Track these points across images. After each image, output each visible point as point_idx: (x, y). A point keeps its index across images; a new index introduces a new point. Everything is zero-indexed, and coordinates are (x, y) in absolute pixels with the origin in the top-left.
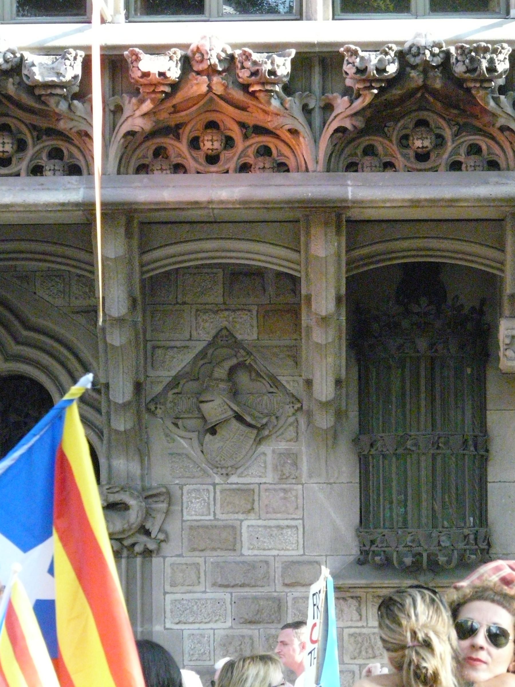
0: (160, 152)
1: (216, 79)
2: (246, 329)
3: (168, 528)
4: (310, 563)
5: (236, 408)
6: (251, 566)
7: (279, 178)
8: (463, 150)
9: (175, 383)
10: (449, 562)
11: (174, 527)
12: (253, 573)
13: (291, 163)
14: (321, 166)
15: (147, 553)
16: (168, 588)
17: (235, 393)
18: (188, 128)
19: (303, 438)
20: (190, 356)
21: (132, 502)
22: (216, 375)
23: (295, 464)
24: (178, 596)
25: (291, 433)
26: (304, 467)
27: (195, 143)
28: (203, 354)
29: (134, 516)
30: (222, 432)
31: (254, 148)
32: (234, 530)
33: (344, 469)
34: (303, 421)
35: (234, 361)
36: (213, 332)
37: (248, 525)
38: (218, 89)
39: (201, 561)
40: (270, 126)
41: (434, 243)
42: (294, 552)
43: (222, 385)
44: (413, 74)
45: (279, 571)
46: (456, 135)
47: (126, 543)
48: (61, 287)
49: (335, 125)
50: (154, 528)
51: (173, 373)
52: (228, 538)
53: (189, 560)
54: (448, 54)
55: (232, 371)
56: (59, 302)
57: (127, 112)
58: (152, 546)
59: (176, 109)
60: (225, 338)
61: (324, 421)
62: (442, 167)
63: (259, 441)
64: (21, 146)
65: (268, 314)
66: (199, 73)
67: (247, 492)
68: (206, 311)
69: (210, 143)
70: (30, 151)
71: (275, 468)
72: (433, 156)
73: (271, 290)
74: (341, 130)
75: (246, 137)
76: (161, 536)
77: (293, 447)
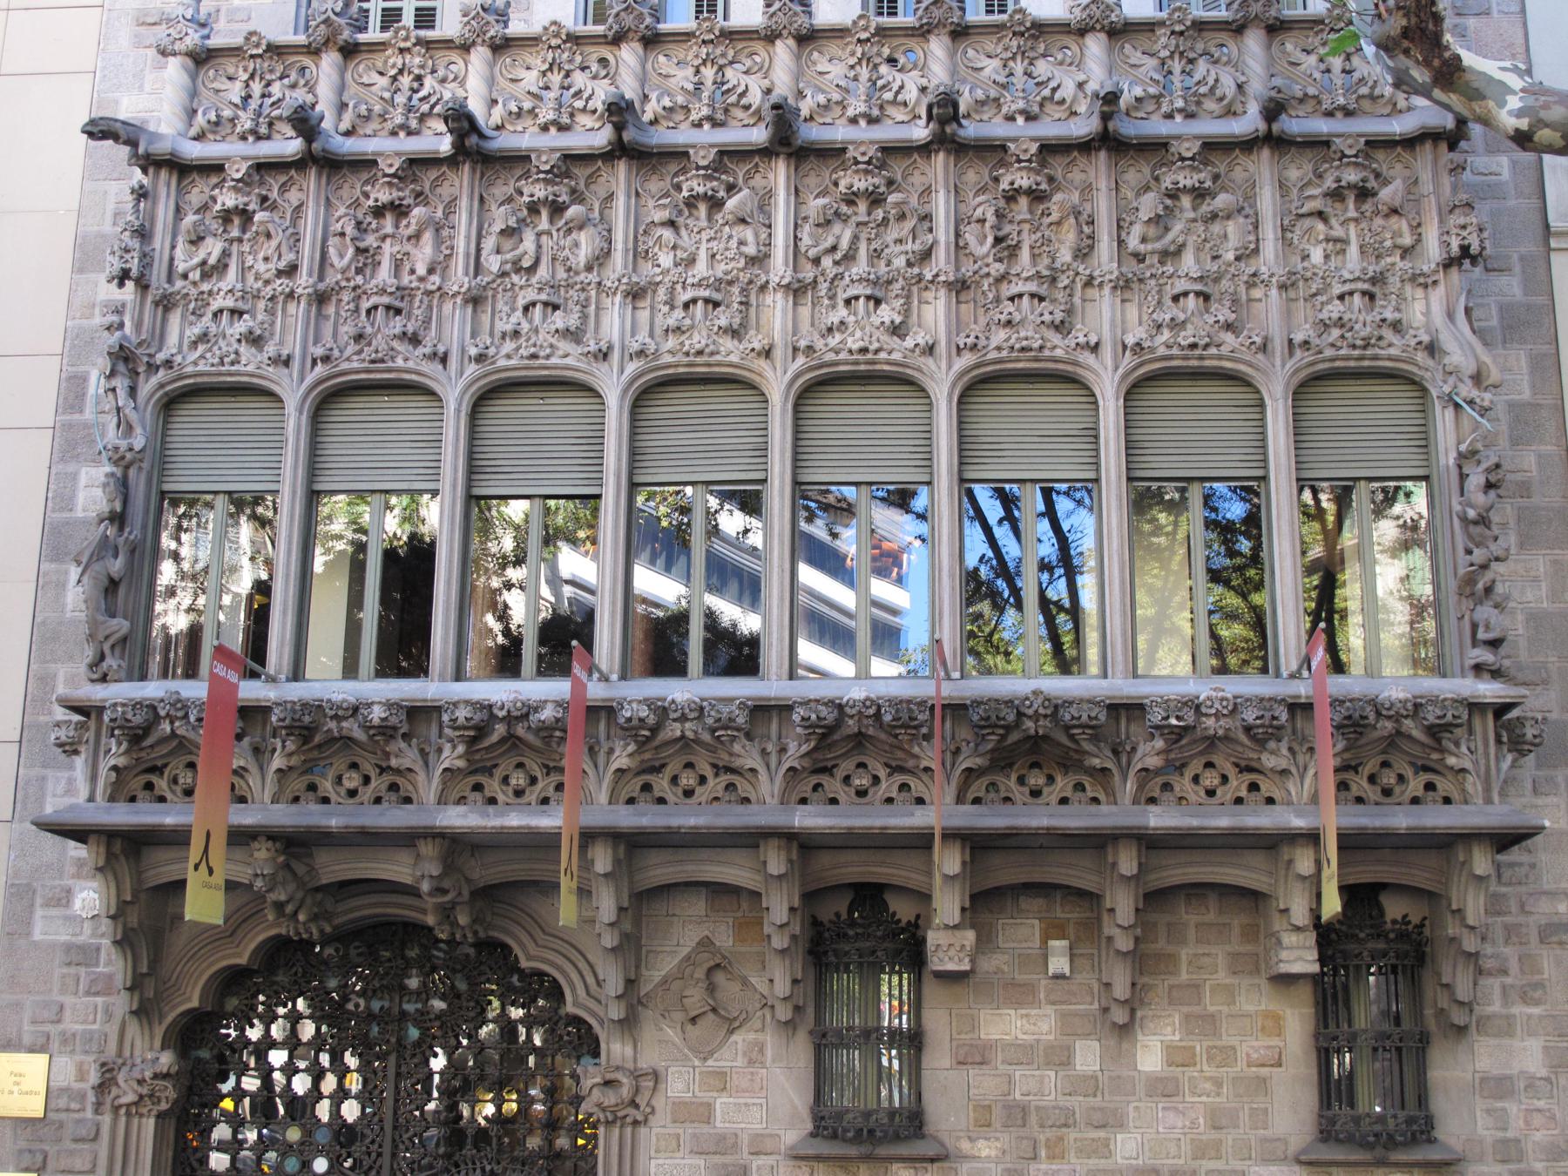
0: (646, 788)
1: (688, 725)
3: (654, 1102)
4: (771, 1135)
6: (722, 1138)
7: (741, 808)
8: (895, 787)
9: (664, 981)
10: (885, 1137)
11: (659, 1102)
12: (724, 1144)
13: (753, 797)
14: (776, 801)
15: (636, 1123)
16: (653, 1154)
17: (712, 989)
19: (768, 1030)
21: (625, 1080)
22: (696, 976)
23: (761, 1051)
24: (661, 1161)
25: (758, 1024)
26: (769, 1053)
27: (674, 780)
28: (688, 958)
29: (625, 1092)
30: (699, 1022)
31: (723, 785)
32: (709, 1107)
33: (801, 1053)
34: (768, 1017)
35: (712, 963)
37: (721, 1102)
38: (690, 734)
39: (681, 1131)
40: (733, 765)
42: (758, 1127)
44: (851, 722)
45: (746, 1142)
46: (890, 775)
47: (620, 1114)
49: (787, 765)
50: (642, 1100)
52: (704, 1113)
53: (671, 1131)
54: (879, 707)
55: (710, 971)
57: (617, 753)
58: (640, 1118)
60: (705, 944)
61: (784, 1013)
62: (877, 803)
63: (731, 1032)
64: (533, 781)
66: (675, 720)
67: (721, 1075)
69: (688, 780)
70: (540, 785)
71: (745, 1054)
72: (871, 792)
74: (791, 769)
75: (717, 775)
76: (648, 1110)
77: (760, 1036)
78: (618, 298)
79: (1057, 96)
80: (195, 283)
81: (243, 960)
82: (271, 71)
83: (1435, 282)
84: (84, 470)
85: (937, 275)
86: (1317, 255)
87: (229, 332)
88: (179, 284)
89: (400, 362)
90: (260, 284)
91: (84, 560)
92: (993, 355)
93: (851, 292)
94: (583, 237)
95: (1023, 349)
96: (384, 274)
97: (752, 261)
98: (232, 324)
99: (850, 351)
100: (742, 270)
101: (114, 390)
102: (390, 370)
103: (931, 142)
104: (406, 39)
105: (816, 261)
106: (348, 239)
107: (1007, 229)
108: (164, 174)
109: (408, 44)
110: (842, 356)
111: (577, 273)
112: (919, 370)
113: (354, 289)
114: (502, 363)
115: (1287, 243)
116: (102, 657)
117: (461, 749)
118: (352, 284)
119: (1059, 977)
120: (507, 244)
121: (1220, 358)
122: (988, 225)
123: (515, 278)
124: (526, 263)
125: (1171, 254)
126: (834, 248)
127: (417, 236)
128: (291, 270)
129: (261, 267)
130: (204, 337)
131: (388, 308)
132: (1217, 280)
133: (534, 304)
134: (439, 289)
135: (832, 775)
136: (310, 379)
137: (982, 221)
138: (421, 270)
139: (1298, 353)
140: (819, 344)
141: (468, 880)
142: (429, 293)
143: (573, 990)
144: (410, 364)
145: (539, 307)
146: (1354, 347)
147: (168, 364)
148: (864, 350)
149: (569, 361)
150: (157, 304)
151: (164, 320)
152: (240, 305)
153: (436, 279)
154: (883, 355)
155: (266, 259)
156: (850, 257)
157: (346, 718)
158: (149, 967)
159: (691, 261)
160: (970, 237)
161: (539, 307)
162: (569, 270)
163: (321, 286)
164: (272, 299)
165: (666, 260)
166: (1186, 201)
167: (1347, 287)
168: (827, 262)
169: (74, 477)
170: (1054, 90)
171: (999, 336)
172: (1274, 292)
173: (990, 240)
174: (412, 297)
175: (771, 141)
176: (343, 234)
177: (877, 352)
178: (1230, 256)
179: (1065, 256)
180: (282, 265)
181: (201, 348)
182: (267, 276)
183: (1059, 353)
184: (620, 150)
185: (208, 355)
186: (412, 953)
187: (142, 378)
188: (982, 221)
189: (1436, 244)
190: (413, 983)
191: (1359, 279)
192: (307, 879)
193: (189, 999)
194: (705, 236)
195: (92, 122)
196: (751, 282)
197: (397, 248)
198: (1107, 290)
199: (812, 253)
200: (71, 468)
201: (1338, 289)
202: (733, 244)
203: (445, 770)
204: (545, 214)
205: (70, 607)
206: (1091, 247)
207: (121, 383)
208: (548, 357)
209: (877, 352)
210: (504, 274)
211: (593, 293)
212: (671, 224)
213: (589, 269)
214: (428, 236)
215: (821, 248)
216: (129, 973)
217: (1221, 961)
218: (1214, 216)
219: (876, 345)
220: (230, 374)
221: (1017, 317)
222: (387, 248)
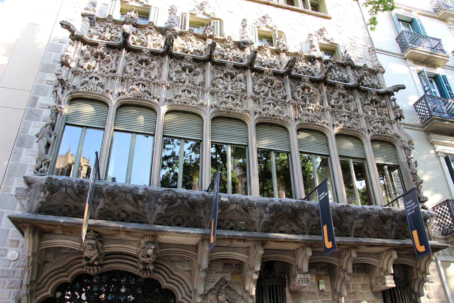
2: (228, 278)
5: (227, 298)
18: (226, 220)
20: (214, 284)
28: (217, 284)
36: (220, 278)
41: (280, 256)
43: (224, 291)
48: (182, 264)
51: (210, 288)
55: (226, 287)
56: (181, 268)
59: (225, 214)
65: (233, 274)
68: (218, 273)
70: (186, 223)
73: (234, 268)
78: (209, 92)
79: (310, 70)
80: (85, 70)
81: (68, 279)
82: (112, 26)
83: (394, 123)
84: (33, 122)
85: (289, 102)
86: (370, 113)
87: (94, 82)
88: (80, 69)
89: (146, 98)
90: (104, 73)
91: (40, 136)
92: (305, 122)
93: (268, 102)
94: (199, 77)
95: (312, 122)
96: (142, 76)
97: (243, 91)
98: (95, 81)
99: (270, 115)
100: (240, 92)
101: (56, 91)
102: (142, 100)
103: (285, 73)
104: (152, 25)
105: (259, 94)
106: (133, 66)
107: (303, 95)
108: (80, 42)
109: (152, 27)
110: (268, 116)
111: (196, 86)
112: (287, 122)
113: (132, 79)
114: (176, 103)
115: (363, 110)
116: (41, 167)
117: (165, 207)
118: (132, 77)
119: (323, 291)
120: (178, 75)
121: (354, 131)
122: (300, 93)
123: (180, 84)
124: (182, 81)
125: (340, 108)
126: (263, 92)
127: (152, 69)
128: (115, 72)
129: (106, 69)
130: (86, 82)
131: (143, 85)
132: (350, 115)
133: (185, 91)
134: (158, 83)
135: (273, 225)
136: (118, 98)
137: (298, 92)
138: (153, 77)
139: (371, 132)
140: (262, 112)
141: (156, 254)
142: (154, 84)
143: (181, 293)
144: (149, 99)
145: (186, 91)
146: (382, 133)
147: (74, 87)
148: (273, 116)
149: (195, 105)
150: (73, 72)
151: (74, 78)
152: (99, 77)
153: (157, 80)
154: (278, 117)
155: (107, 67)
156: (266, 95)
157: (128, 193)
158: (36, 278)
159: (226, 88)
160: (296, 95)
161: (186, 91)
162: (194, 84)
163: (124, 76)
164: (107, 78)
165: (221, 86)
166: (341, 97)
167: (378, 120)
168: (262, 94)
169: (30, 124)
170: (309, 69)
171: (306, 118)
172: (363, 119)
173: (301, 96)
174: (149, 84)
175: (248, 64)
176: (131, 64)
177: (277, 116)
178: (353, 110)
179: (318, 104)
180: (112, 69)
181: (85, 85)
182: (107, 71)
183: (320, 124)
184: (210, 59)
185: (87, 87)
186: (123, 281)
187: (66, 90)
188: (298, 92)
189: (393, 115)
190: (123, 290)
191: (380, 119)
192: (100, 249)
193: (47, 291)
194: (230, 83)
195: (63, 21)
196: (242, 96)
197: (146, 71)
198: (328, 112)
199: (258, 91)
200: (29, 121)
201: (375, 121)
202: (239, 85)
203: (158, 214)
204: (187, 71)
205: (22, 160)
206: (322, 103)
207: (60, 89)
208: (189, 103)
209: (277, 116)
210: (176, 82)
211: (200, 91)
212: (222, 78)
213: (199, 85)
214: (156, 69)
215: (261, 90)
216: (29, 279)
217: (360, 286)
218: (348, 101)
219: (276, 115)
220: (93, 94)
221: (310, 114)
222: (143, 70)
